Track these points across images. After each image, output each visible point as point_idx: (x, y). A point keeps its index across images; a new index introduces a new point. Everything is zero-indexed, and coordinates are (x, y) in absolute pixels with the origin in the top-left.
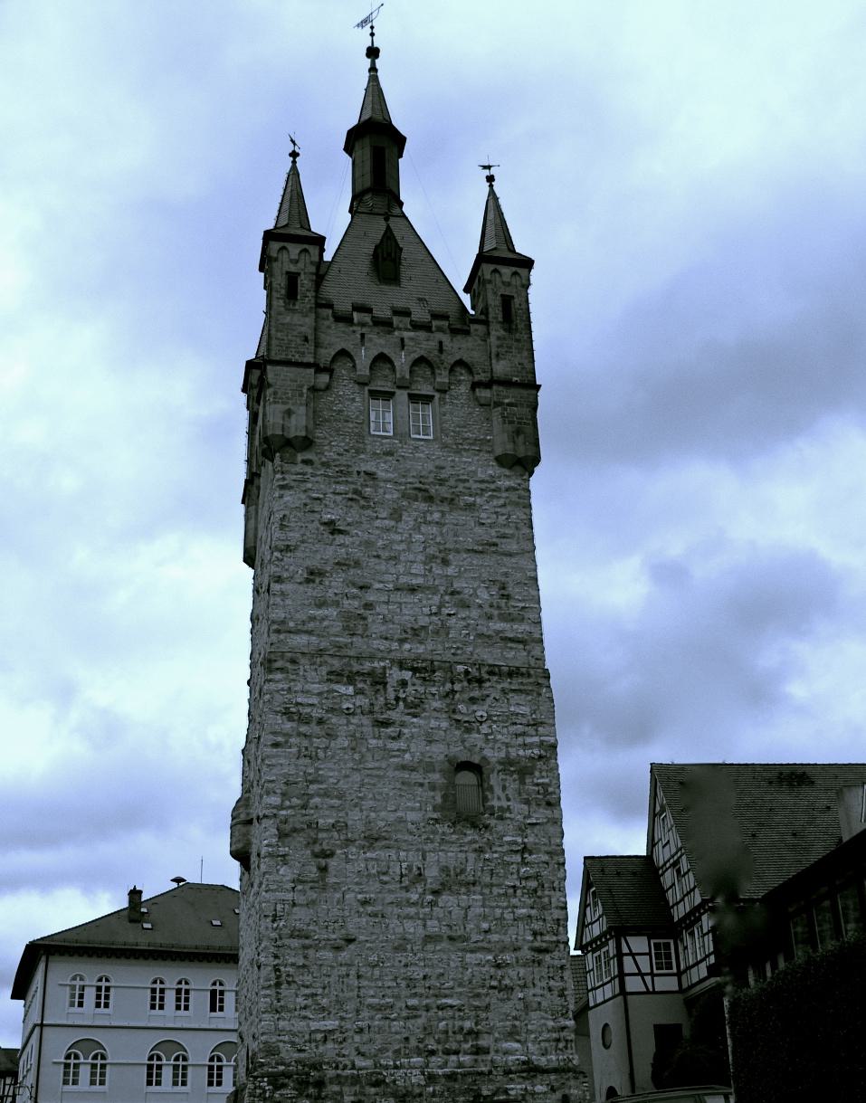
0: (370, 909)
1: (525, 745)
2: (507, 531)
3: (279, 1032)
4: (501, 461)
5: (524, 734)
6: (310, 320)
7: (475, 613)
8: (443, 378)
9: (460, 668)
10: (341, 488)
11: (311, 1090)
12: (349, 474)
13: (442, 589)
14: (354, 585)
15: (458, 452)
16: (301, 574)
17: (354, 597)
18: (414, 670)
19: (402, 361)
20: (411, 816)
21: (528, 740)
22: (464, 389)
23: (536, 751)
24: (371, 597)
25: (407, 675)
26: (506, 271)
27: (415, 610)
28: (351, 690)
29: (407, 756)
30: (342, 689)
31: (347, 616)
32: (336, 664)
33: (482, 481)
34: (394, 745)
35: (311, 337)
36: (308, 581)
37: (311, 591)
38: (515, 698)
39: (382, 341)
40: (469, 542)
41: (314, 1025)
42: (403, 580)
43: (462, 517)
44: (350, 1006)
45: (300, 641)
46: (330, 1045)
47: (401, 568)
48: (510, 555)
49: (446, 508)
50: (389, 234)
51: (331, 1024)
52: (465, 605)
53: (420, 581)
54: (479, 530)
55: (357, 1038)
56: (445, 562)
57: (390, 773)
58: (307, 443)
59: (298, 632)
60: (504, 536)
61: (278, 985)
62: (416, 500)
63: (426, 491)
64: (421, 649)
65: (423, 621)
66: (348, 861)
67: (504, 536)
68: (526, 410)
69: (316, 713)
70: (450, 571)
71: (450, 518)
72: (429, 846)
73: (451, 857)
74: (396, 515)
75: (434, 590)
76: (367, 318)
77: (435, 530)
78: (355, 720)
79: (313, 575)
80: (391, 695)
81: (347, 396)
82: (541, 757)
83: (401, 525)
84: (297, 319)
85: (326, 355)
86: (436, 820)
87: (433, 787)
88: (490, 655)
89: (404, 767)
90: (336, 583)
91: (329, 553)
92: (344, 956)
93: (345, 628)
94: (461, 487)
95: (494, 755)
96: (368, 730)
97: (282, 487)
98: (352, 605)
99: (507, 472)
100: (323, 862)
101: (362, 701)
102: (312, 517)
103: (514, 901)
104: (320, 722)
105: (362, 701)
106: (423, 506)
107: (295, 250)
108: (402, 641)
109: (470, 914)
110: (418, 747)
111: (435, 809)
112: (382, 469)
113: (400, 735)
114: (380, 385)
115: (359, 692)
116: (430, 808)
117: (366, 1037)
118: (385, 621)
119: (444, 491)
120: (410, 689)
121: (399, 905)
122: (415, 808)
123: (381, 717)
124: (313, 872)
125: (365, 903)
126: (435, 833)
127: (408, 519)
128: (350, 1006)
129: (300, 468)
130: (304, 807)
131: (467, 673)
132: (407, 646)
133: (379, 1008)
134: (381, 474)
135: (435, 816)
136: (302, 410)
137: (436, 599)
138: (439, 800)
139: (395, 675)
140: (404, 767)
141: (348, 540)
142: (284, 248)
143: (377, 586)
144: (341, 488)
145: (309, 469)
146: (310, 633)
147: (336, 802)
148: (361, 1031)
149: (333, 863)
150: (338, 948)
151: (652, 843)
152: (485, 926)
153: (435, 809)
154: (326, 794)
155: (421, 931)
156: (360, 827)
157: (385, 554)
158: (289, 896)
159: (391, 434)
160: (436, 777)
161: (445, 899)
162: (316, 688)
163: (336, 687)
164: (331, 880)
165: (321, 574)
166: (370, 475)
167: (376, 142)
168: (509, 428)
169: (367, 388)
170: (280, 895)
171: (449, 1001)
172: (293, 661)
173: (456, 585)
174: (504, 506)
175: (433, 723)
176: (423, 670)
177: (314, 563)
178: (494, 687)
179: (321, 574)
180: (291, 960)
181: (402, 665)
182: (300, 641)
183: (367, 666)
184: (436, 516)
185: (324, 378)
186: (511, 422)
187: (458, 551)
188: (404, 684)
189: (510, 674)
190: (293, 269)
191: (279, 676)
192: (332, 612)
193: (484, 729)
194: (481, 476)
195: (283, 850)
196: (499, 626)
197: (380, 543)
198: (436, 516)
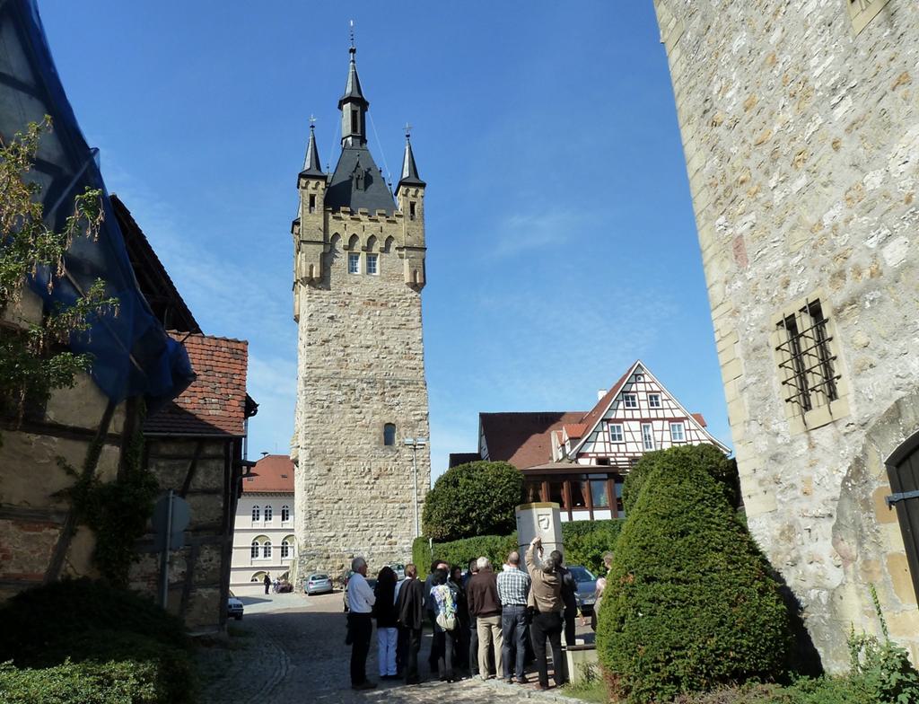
0: (348, 486)
1: (415, 415)
2: (410, 318)
5: (414, 410)
6: (322, 219)
7: (394, 356)
9: (388, 382)
11: (324, 560)
13: (380, 346)
17: (342, 351)
20: (365, 446)
21: (416, 412)
23: (418, 417)
26: (412, 190)
27: (369, 356)
28: (340, 393)
29: (364, 421)
30: (336, 393)
32: (335, 382)
34: (359, 416)
35: (322, 228)
36: (322, 345)
37: (322, 349)
38: (411, 394)
39: (354, 228)
40: (391, 324)
41: (325, 534)
43: (386, 312)
44: (340, 526)
46: (331, 542)
48: (412, 329)
49: (382, 308)
51: (332, 534)
54: (397, 318)
56: (383, 334)
59: (318, 368)
60: (408, 321)
63: (374, 301)
67: (408, 321)
68: (420, 261)
70: (384, 337)
72: (373, 459)
73: (381, 463)
74: (360, 313)
76: (348, 216)
77: (377, 318)
80: (358, 395)
82: (421, 420)
83: (363, 317)
84: (315, 218)
86: (376, 448)
87: (375, 434)
88: (400, 375)
90: (333, 346)
93: (338, 365)
95: (401, 420)
97: (309, 301)
99: (411, 290)
100: (328, 467)
101: (344, 397)
102: (323, 314)
103: (408, 481)
104: (328, 407)
105: (344, 397)
106: (373, 308)
107: (313, 183)
108: (363, 370)
109: (390, 487)
110: (368, 417)
111: (375, 444)
112: (353, 290)
113: (361, 413)
115: (346, 394)
116: (373, 442)
117: (345, 538)
118: (355, 361)
119: (383, 300)
120: (366, 392)
121: (360, 484)
122: (367, 442)
123: (353, 405)
124: (325, 472)
125: (346, 484)
126: (375, 454)
130: (321, 444)
131: (390, 384)
132: (364, 373)
133: (352, 527)
134: (354, 293)
135: (376, 446)
136: (319, 264)
138: (377, 439)
140: (363, 426)
141: (338, 325)
146: (322, 368)
147: (334, 442)
148: (344, 536)
149: (333, 467)
150: (335, 503)
151: (480, 448)
152: (395, 492)
153: (375, 444)
154: (331, 439)
155: (369, 495)
156: (344, 451)
158: (315, 481)
160: (376, 430)
161: (381, 481)
162: (325, 393)
163: (333, 392)
165: (327, 341)
166: (350, 294)
168: (413, 269)
170: (310, 481)
171: (380, 524)
173: (387, 344)
174: (409, 306)
175: (375, 406)
176: (372, 382)
177: (325, 336)
178: (402, 390)
183: (348, 382)
186: (413, 267)
187: (388, 328)
188: (363, 389)
189: (409, 384)
190: (313, 192)
191: (309, 387)
193: (397, 408)
195: (312, 463)
196: (405, 362)
197: (354, 326)
198: (378, 312)
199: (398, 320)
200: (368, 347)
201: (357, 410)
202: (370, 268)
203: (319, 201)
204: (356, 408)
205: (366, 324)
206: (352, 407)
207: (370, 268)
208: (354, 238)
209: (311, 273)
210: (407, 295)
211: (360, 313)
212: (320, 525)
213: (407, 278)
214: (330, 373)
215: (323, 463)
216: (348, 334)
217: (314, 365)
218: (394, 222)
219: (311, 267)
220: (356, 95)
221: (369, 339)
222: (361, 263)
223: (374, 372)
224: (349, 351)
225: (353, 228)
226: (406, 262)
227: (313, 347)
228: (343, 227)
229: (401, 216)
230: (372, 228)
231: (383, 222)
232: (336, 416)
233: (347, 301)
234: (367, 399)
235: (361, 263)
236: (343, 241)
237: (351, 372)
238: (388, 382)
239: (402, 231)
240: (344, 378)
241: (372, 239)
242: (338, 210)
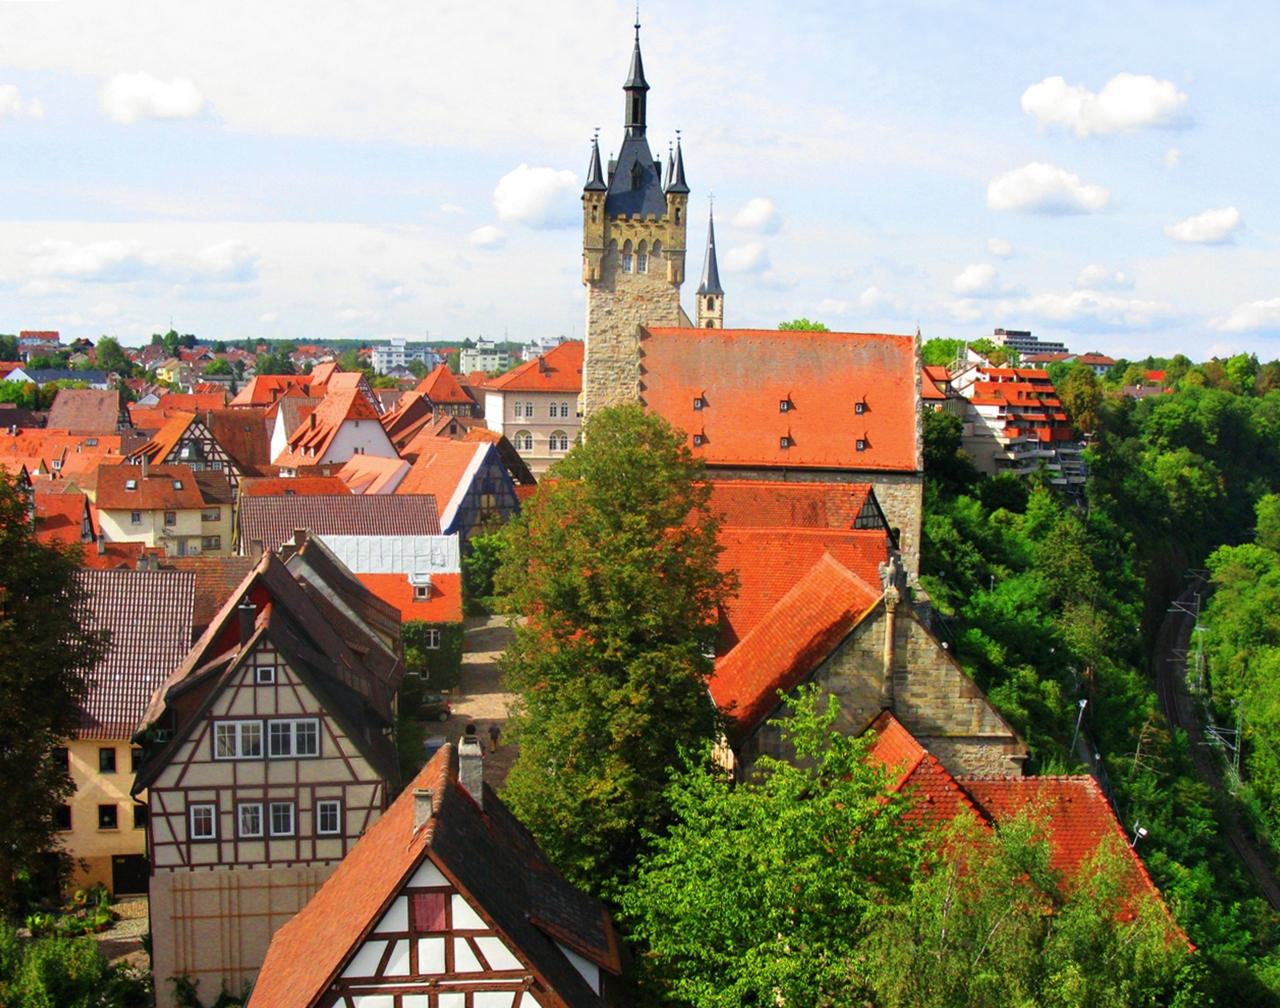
4: (671, 283)
6: (602, 228)
31: (613, 347)
37: (600, 338)
74: (630, 307)
79: (604, 331)
90: (608, 335)
112: (626, 288)
119: (649, 296)
127: (633, 311)
167: (638, 91)
177: (603, 328)
190: (595, 203)
199: (661, 312)
202: (640, 268)
203: (600, 209)
207: (640, 268)
208: (628, 242)
209: (593, 275)
210: (670, 292)
211: (630, 307)
213: (669, 278)
214: (605, 357)
216: (620, 325)
219: (593, 271)
220: (640, 85)
222: (633, 264)
224: (620, 339)
225: (627, 234)
226: (669, 263)
228: (621, 234)
229: (667, 221)
230: (643, 233)
231: (653, 229)
232: (609, 390)
235: (633, 264)
236: (620, 246)
237: (622, 356)
239: (666, 237)
240: (617, 361)
241: (642, 243)
242: (616, 218)
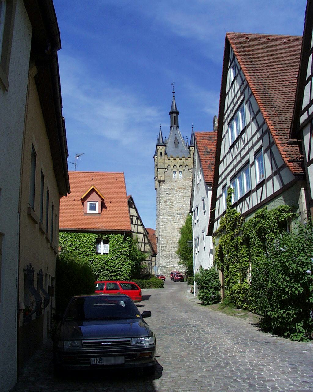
0: (173, 247)
3: (162, 262)
8: (184, 168)
10: (169, 188)
12: (170, 185)
14: (171, 203)
15: (186, 180)
16: (164, 201)
18: (179, 215)
19: (178, 166)
22: (187, 170)
24: (173, 204)
25: (178, 215)
30: (169, 218)
31: (170, 207)
32: (169, 214)
33: (189, 185)
36: (165, 202)
39: (175, 162)
42: (178, 201)
43: (186, 191)
45: (164, 211)
46: (168, 263)
47: (177, 200)
49: (184, 190)
50: (176, 141)
51: (168, 261)
52: (186, 205)
53: (180, 202)
55: (172, 262)
56: (184, 198)
57: (176, 229)
58: (164, 181)
59: (163, 210)
61: (162, 256)
62: (179, 189)
64: (180, 212)
65: (181, 207)
66: (170, 241)
69: (166, 221)
70: (184, 200)
71: (184, 191)
74: (177, 192)
75: (182, 203)
76: (172, 158)
77: (182, 193)
78: (171, 222)
81: (170, 172)
83: (178, 193)
85: (166, 165)
89: (177, 228)
91: (168, 198)
92: (170, 253)
93: (170, 209)
94: (186, 186)
96: (173, 223)
98: (171, 205)
101: (172, 219)
102: (165, 192)
105: (172, 219)
106: (180, 190)
107: (161, 147)
114: (174, 170)
115: (172, 218)
119: (184, 187)
120: (178, 217)
124: (166, 242)
127: (178, 192)
128: (171, 259)
129: (163, 185)
132: (178, 211)
137: (182, 204)
139: (177, 215)
140: (177, 228)
142: (160, 147)
143: (174, 202)
144: (169, 188)
145: (164, 185)
146: (165, 210)
149: (168, 241)
157: (175, 198)
158: (163, 245)
159: (176, 178)
162: (166, 218)
164: (168, 243)
169: (173, 171)
172: (163, 214)
175: (181, 222)
179: (166, 201)
180: (163, 253)
181: (177, 214)
182: (164, 211)
184: (183, 191)
185: (166, 170)
188: (178, 217)
191: (161, 216)
192: (168, 207)
194: (189, 184)
195: (162, 240)
197: (175, 196)
198: (183, 191)
200: (179, 203)
201: (176, 223)
203: (163, 153)
204: (175, 222)
205: (178, 195)
206: (174, 222)
212: (165, 258)
215: (165, 240)
217: (163, 209)
218: (188, 160)
221: (179, 200)
223: (181, 211)
227: (162, 203)
233: (173, 188)
234: (178, 220)
237: (174, 211)
238: (185, 214)
